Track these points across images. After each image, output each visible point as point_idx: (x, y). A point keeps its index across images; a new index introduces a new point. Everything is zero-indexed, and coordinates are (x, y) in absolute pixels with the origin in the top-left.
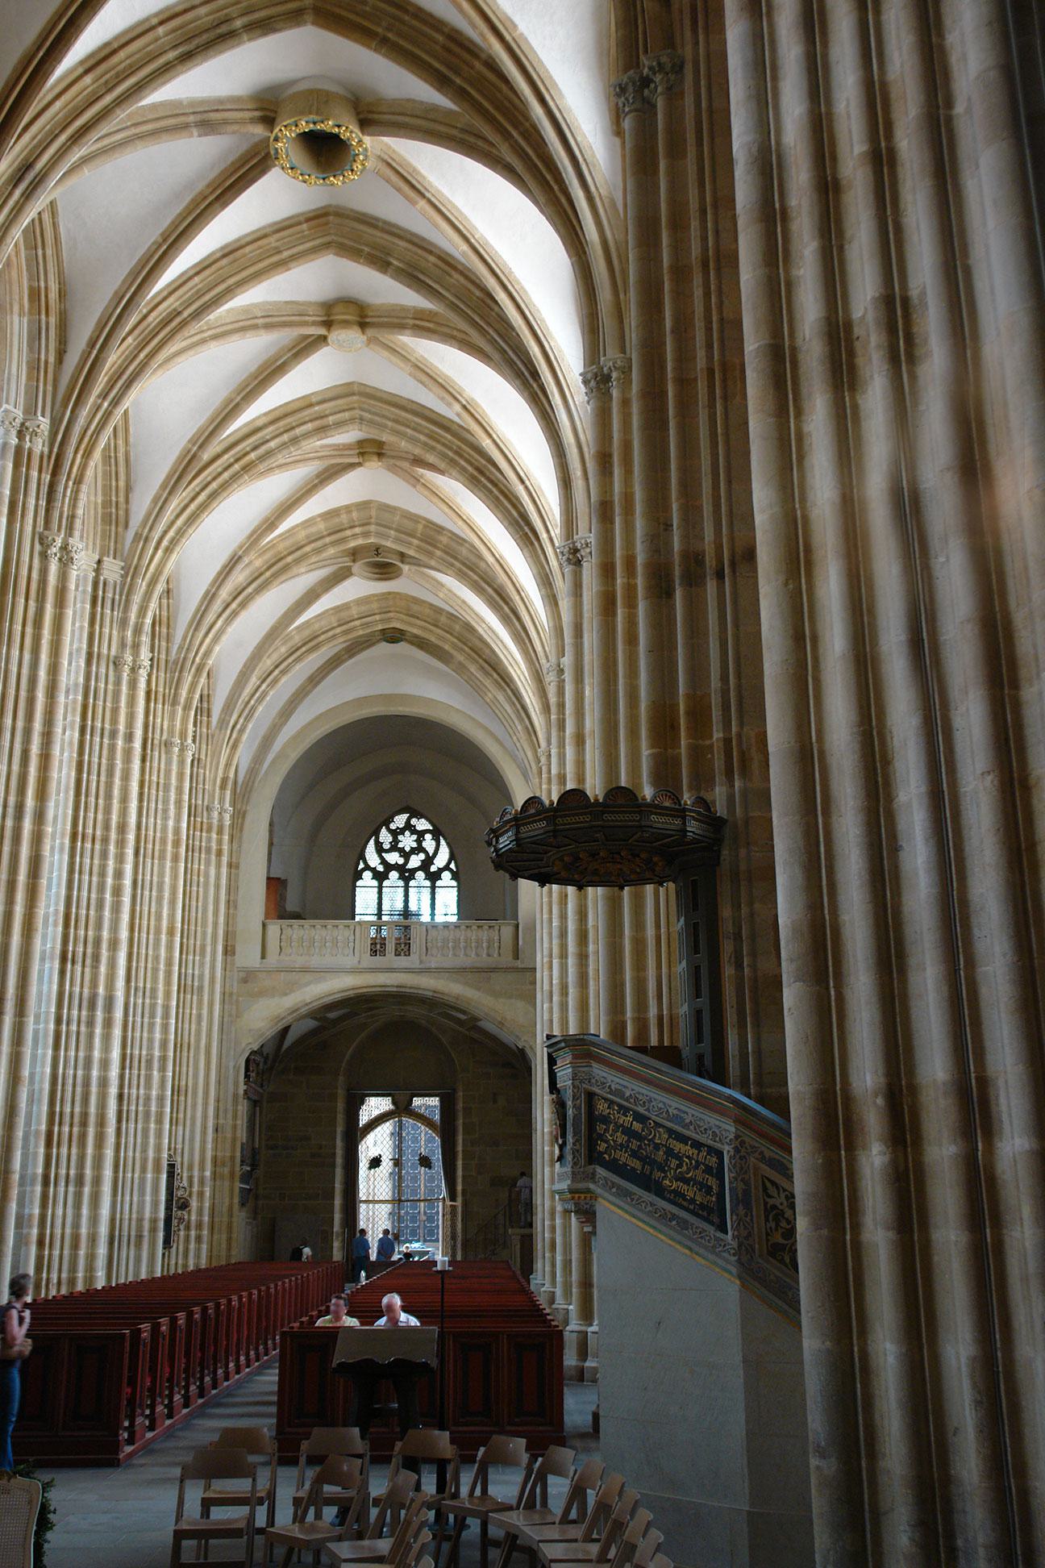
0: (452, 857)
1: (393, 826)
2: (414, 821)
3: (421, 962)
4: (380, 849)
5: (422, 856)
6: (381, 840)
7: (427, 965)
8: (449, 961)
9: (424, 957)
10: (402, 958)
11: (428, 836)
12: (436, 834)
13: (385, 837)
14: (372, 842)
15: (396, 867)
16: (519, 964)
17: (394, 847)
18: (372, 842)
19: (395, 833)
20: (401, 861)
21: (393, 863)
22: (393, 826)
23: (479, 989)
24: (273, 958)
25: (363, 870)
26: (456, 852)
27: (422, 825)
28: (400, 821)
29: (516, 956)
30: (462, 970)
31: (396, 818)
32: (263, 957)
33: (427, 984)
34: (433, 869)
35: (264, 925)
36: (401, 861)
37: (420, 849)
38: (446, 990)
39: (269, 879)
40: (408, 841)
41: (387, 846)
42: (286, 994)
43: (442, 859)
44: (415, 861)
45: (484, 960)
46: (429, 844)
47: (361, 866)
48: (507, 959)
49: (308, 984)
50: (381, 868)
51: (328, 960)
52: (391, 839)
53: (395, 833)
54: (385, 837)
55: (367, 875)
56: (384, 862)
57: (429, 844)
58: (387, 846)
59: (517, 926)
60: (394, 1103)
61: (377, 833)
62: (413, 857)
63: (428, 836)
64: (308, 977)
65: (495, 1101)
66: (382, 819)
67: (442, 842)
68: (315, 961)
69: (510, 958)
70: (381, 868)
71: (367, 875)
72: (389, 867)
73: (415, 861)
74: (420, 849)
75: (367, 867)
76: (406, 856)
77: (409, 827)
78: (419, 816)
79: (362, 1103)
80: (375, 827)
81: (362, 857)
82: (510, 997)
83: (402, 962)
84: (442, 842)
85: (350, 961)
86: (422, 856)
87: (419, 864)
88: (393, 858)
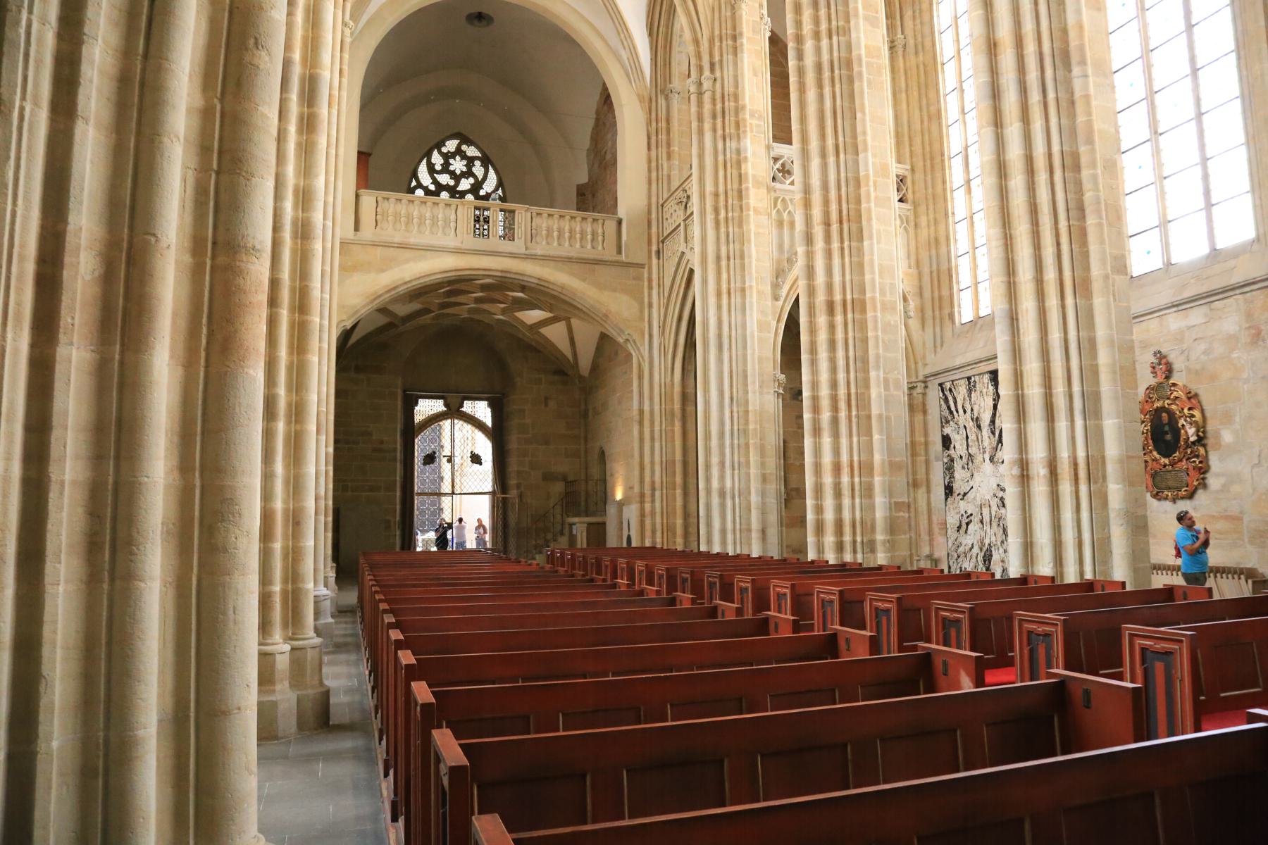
0: (500, 184)
1: (444, 150)
2: (464, 147)
3: (526, 249)
4: (431, 169)
5: (471, 180)
6: (433, 161)
7: (533, 252)
8: (554, 249)
9: (529, 244)
10: (507, 242)
11: (477, 163)
12: (486, 162)
13: (437, 160)
14: (424, 162)
15: (446, 188)
16: (623, 257)
17: (446, 169)
18: (424, 162)
19: (447, 157)
20: (452, 183)
21: (444, 183)
22: (444, 150)
23: (584, 280)
24: (367, 231)
25: (416, 188)
26: (504, 180)
27: (471, 151)
28: (451, 145)
29: (619, 252)
30: (569, 260)
31: (448, 143)
32: (357, 228)
33: (533, 271)
34: (482, 193)
35: (357, 196)
36: (452, 183)
37: (469, 173)
38: (552, 279)
39: (359, 153)
40: (458, 165)
41: (438, 168)
42: (383, 271)
43: (489, 186)
44: (465, 184)
45: (588, 252)
46: (478, 170)
47: (414, 183)
48: (610, 255)
49: (407, 261)
50: (432, 188)
51: (426, 239)
52: (442, 161)
53: (447, 157)
54: (437, 160)
55: (420, 192)
56: (435, 182)
57: (478, 170)
58: (438, 168)
59: (620, 222)
60: (446, 405)
61: (428, 155)
62: (463, 181)
63: (477, 163)
64: (408, 254)
65: (546, 405)
66: (432, 144)
67: (490, 168)
68: (414, 239)
69: (615, 252)
70: (432, 188)
71: (420, 192)
72: (440, 187)
73: (465, 184)
74: (469, 173)
75: (420, 185)
76: (457, 178)
77: (459, 152)
78: (469, 142)
79: (416, 404)
80: (427, 148)
81: (415, 175)
82: (615, 290)
83: (507, 246)
84: (490, 168)
85: (450, 241)
86: (471, 180)
87: (469, 187)
88: (444, 179)
